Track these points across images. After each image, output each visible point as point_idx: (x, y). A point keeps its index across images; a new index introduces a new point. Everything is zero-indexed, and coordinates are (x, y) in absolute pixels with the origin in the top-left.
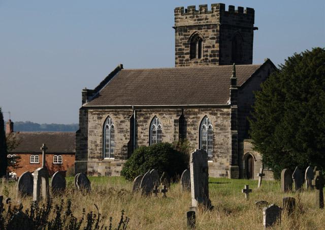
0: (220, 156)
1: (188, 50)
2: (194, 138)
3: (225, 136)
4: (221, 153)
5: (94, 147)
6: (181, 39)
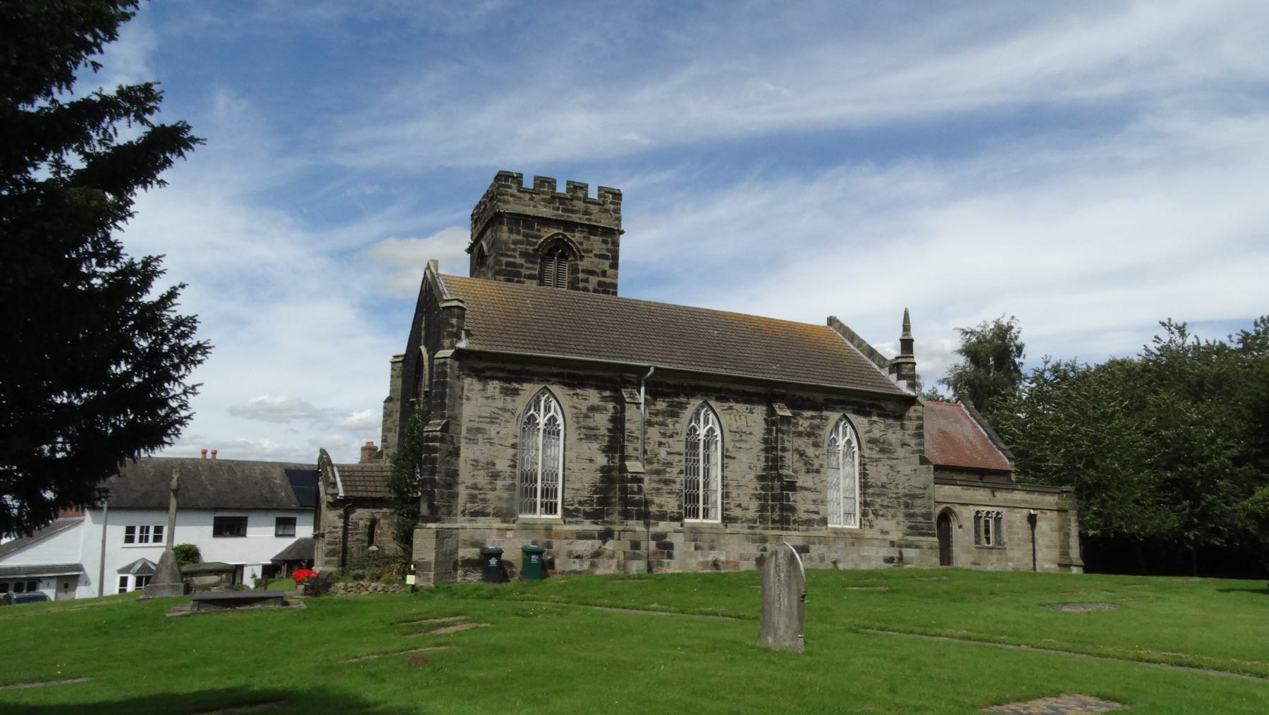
0: (881, 513)
1: (535, 269)
2: (816, 467)
3: (892, 467)
4: (881, 506)
5: (482, 479)
6: (515, 243)
